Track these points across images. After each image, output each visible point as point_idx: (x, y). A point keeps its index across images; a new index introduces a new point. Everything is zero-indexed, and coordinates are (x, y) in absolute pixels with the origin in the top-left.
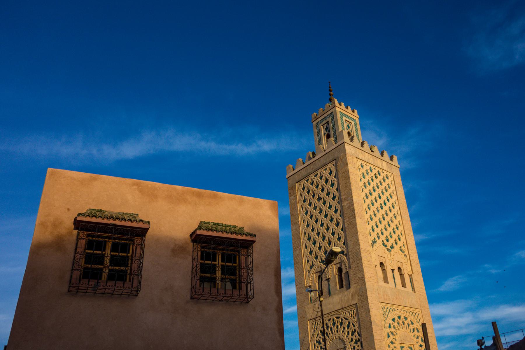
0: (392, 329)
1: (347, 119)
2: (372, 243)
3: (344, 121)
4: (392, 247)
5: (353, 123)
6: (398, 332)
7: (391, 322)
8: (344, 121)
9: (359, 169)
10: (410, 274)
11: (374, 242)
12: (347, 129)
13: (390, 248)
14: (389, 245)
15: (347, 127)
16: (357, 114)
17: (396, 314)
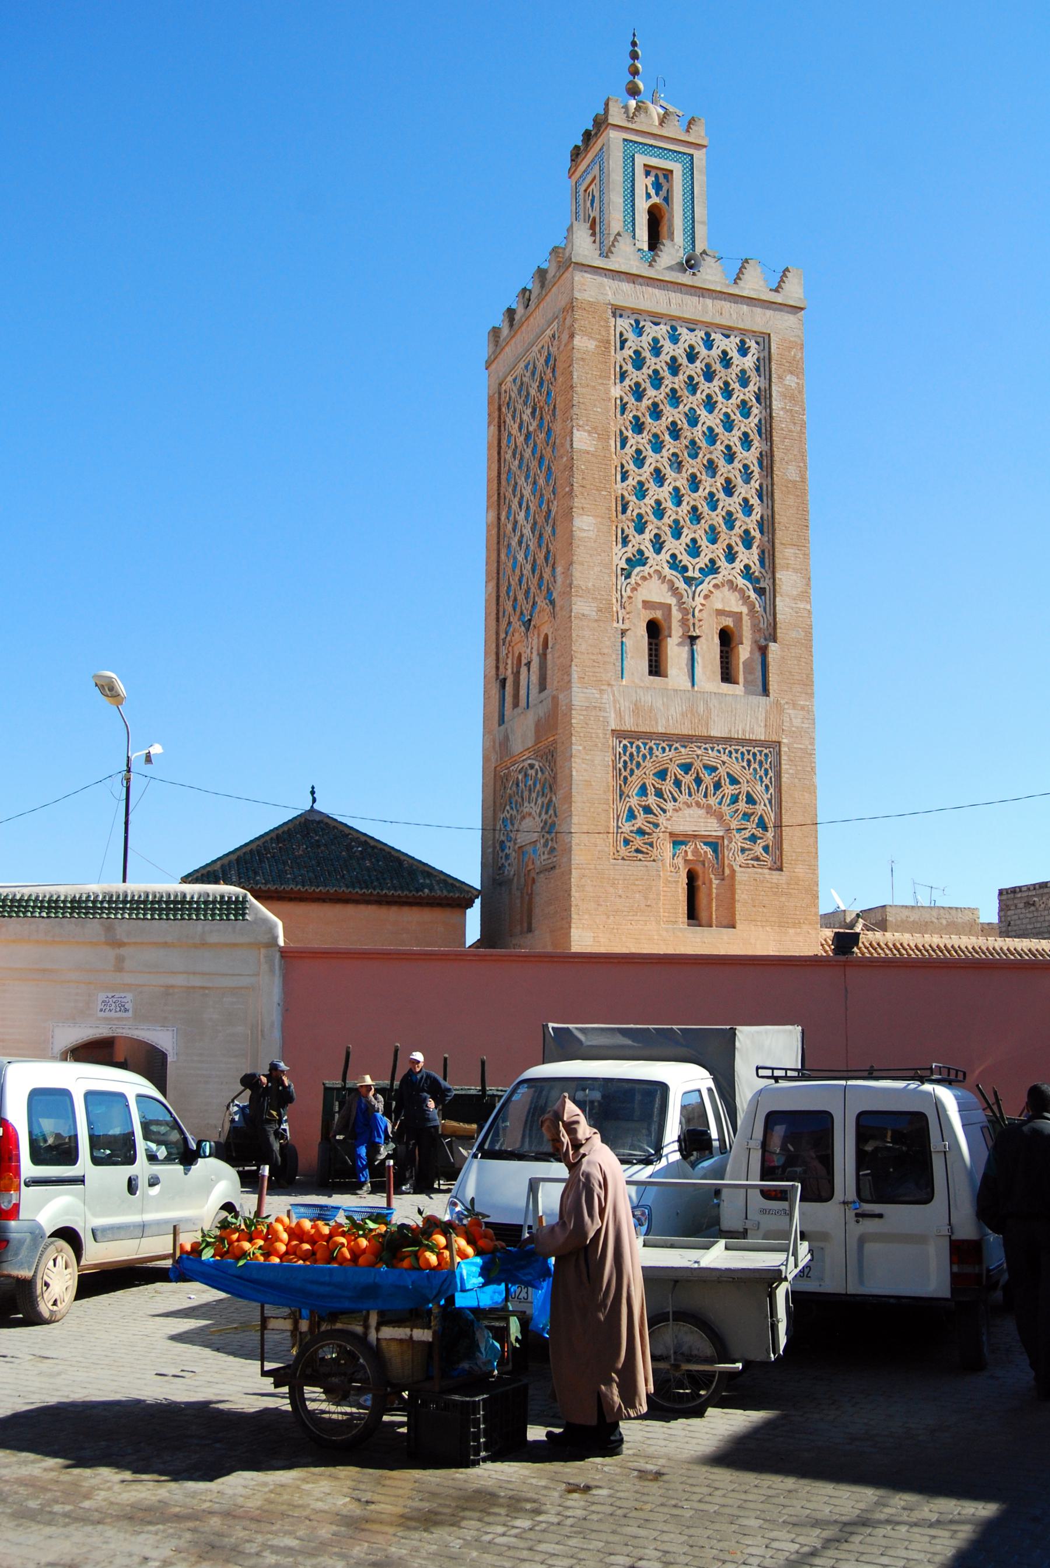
0: (652, 800)
1: (654, 162)
2: (626, 566)
3: (639, 171)
4: (712, 568)
5: (677, 169)
6: (669, 806)
7: (650, 781)
8: (639, 171)
9: (623, 342)
10: (763, 643)
11: (638, 560)
12: (649, 196)
13: (697, 574)
14: (694, 566)
15: (650, 187)
16: (703, 134)
17: (674, 759)
